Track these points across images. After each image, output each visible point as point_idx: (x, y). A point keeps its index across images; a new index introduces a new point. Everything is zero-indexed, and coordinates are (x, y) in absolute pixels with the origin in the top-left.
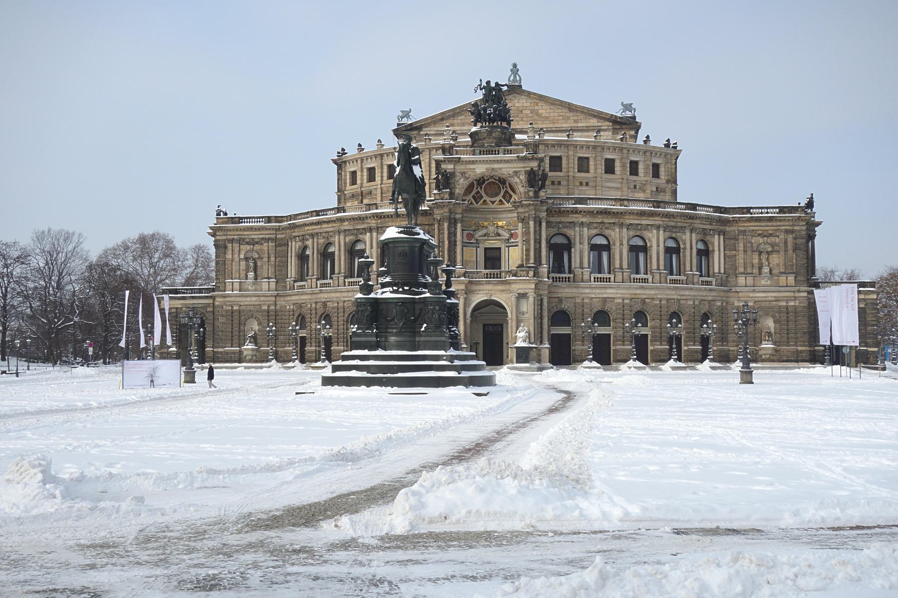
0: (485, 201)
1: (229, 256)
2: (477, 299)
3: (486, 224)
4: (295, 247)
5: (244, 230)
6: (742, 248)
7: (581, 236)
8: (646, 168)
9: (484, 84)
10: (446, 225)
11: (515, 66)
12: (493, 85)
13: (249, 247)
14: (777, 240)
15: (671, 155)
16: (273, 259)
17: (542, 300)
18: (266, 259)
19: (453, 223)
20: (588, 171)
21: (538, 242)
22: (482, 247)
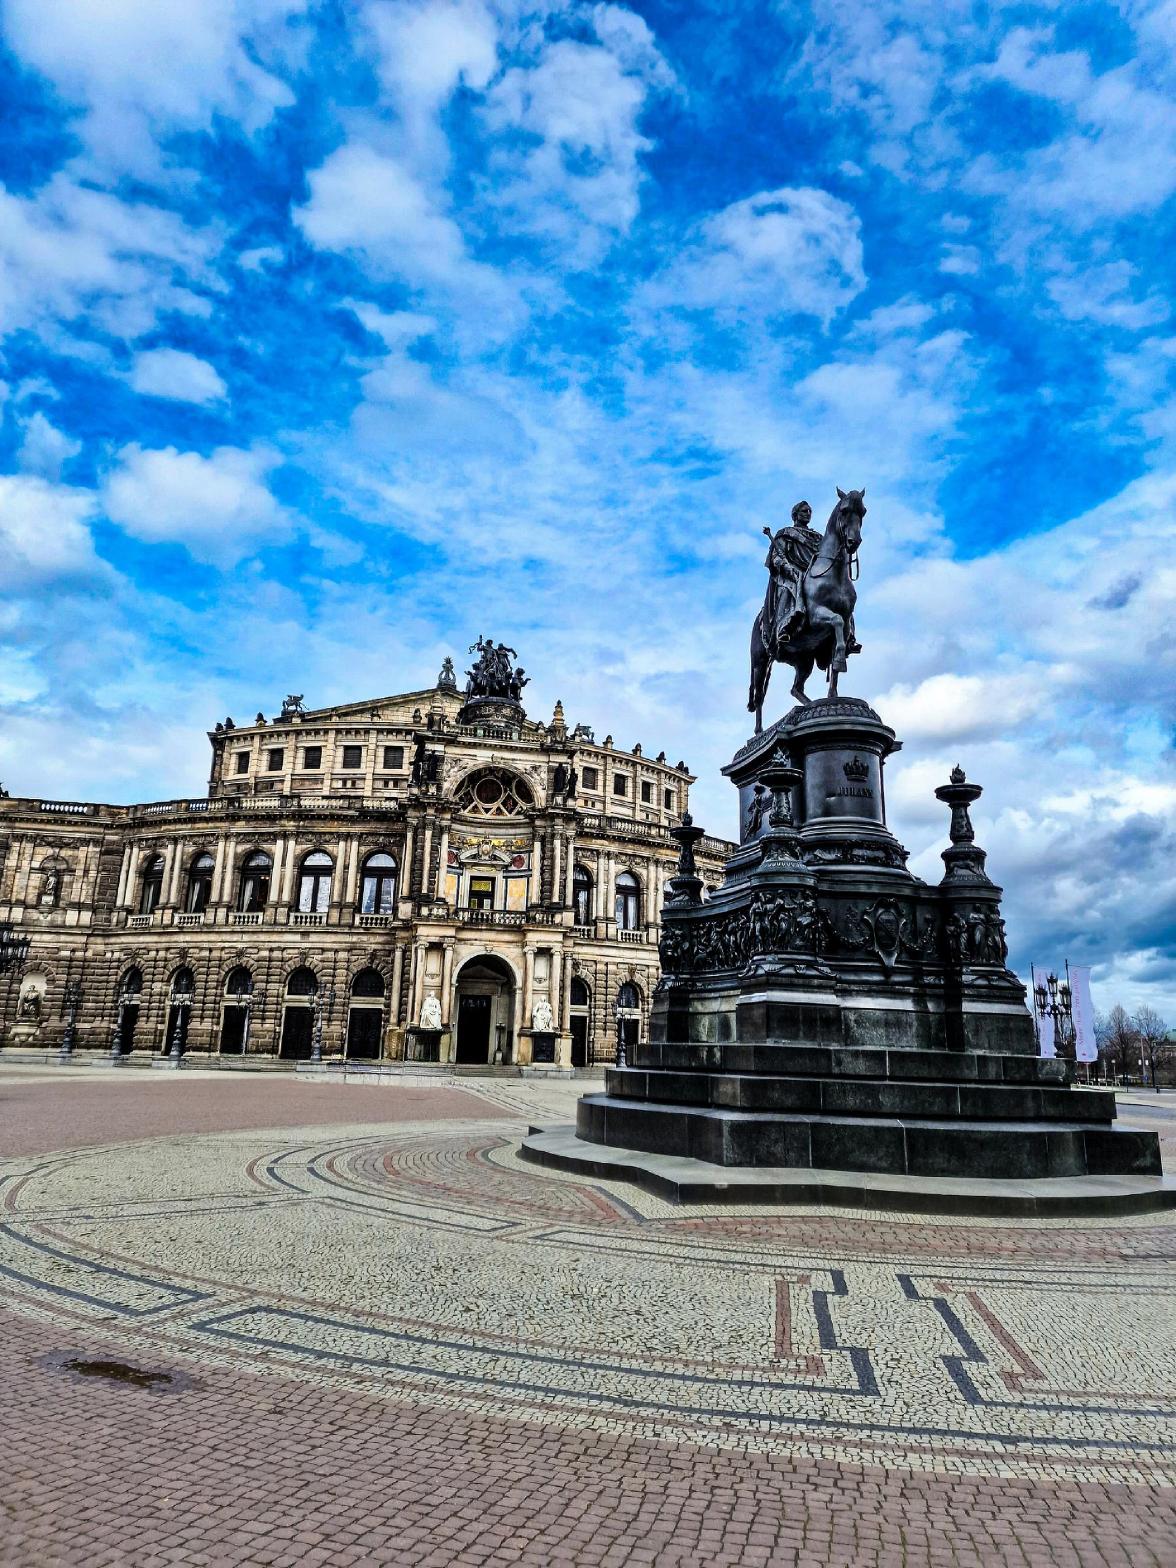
1: (12, 862)
2: (468, 952)
4: (135, 857)
5: (49, 822)
7: (607, 871)
8: (659, 795)
10: (429, 834)
11: (448, 661)
13: (50, 851)
16: (92, 874)
18: (79, 873)
19: (439, 832)
22: (468, 873)
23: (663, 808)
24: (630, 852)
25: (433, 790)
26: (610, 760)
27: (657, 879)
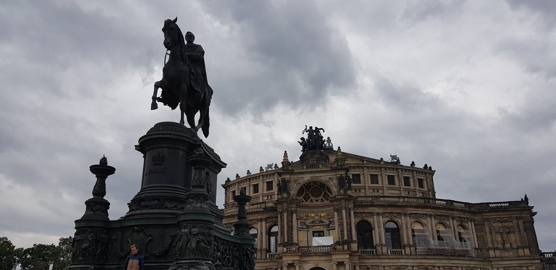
0: (312, 200)
3: (313, 215)
6: (487, 230)
7: (379, 223)
8: (414, 182)
9: (308, 128)
10: (285, 214)
12: (314, 129)
14: (511, 224)
15: (430, 174)
17: (355, 267)
20: (378, 183)
21: (349, 224)
23: (417, 188)
24: (390, 212)
25: (285, 195)
26: (383, 169)
27: (407, 223)
